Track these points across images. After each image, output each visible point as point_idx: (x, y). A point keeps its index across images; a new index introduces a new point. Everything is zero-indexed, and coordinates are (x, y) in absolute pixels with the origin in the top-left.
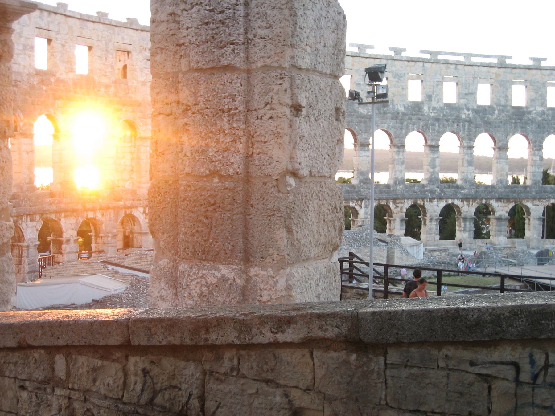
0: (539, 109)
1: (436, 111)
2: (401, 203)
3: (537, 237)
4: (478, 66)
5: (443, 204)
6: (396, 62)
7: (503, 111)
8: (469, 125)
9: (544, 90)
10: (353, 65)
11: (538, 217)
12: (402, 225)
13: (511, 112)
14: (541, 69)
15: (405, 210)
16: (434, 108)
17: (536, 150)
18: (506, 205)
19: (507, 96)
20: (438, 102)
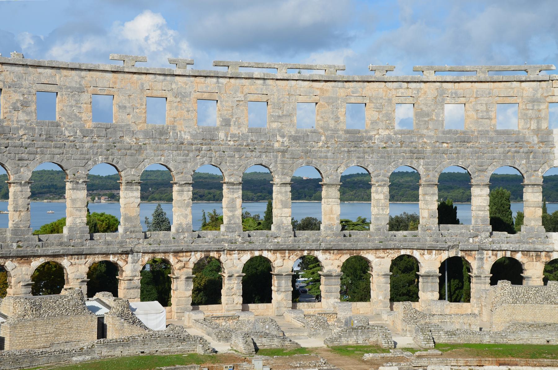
0: (384, 133)
1: (236, 139)
2: (186, 256)
3: (382, 299)
4: (297, 80)
5: (246, 257)
6: (177, 78)
7: (332, 137)
8: (283, 156)
9: (390, 109)
10: (115, 83)
11: (383, 273)
12: (187, 285)
13: (343, 138)
14: (385, 82)
15: (191, 265)
16: (233, 136)
17: (379, 186)
18: (338, 257)
19: (339, 118)
20: (239, 128)
